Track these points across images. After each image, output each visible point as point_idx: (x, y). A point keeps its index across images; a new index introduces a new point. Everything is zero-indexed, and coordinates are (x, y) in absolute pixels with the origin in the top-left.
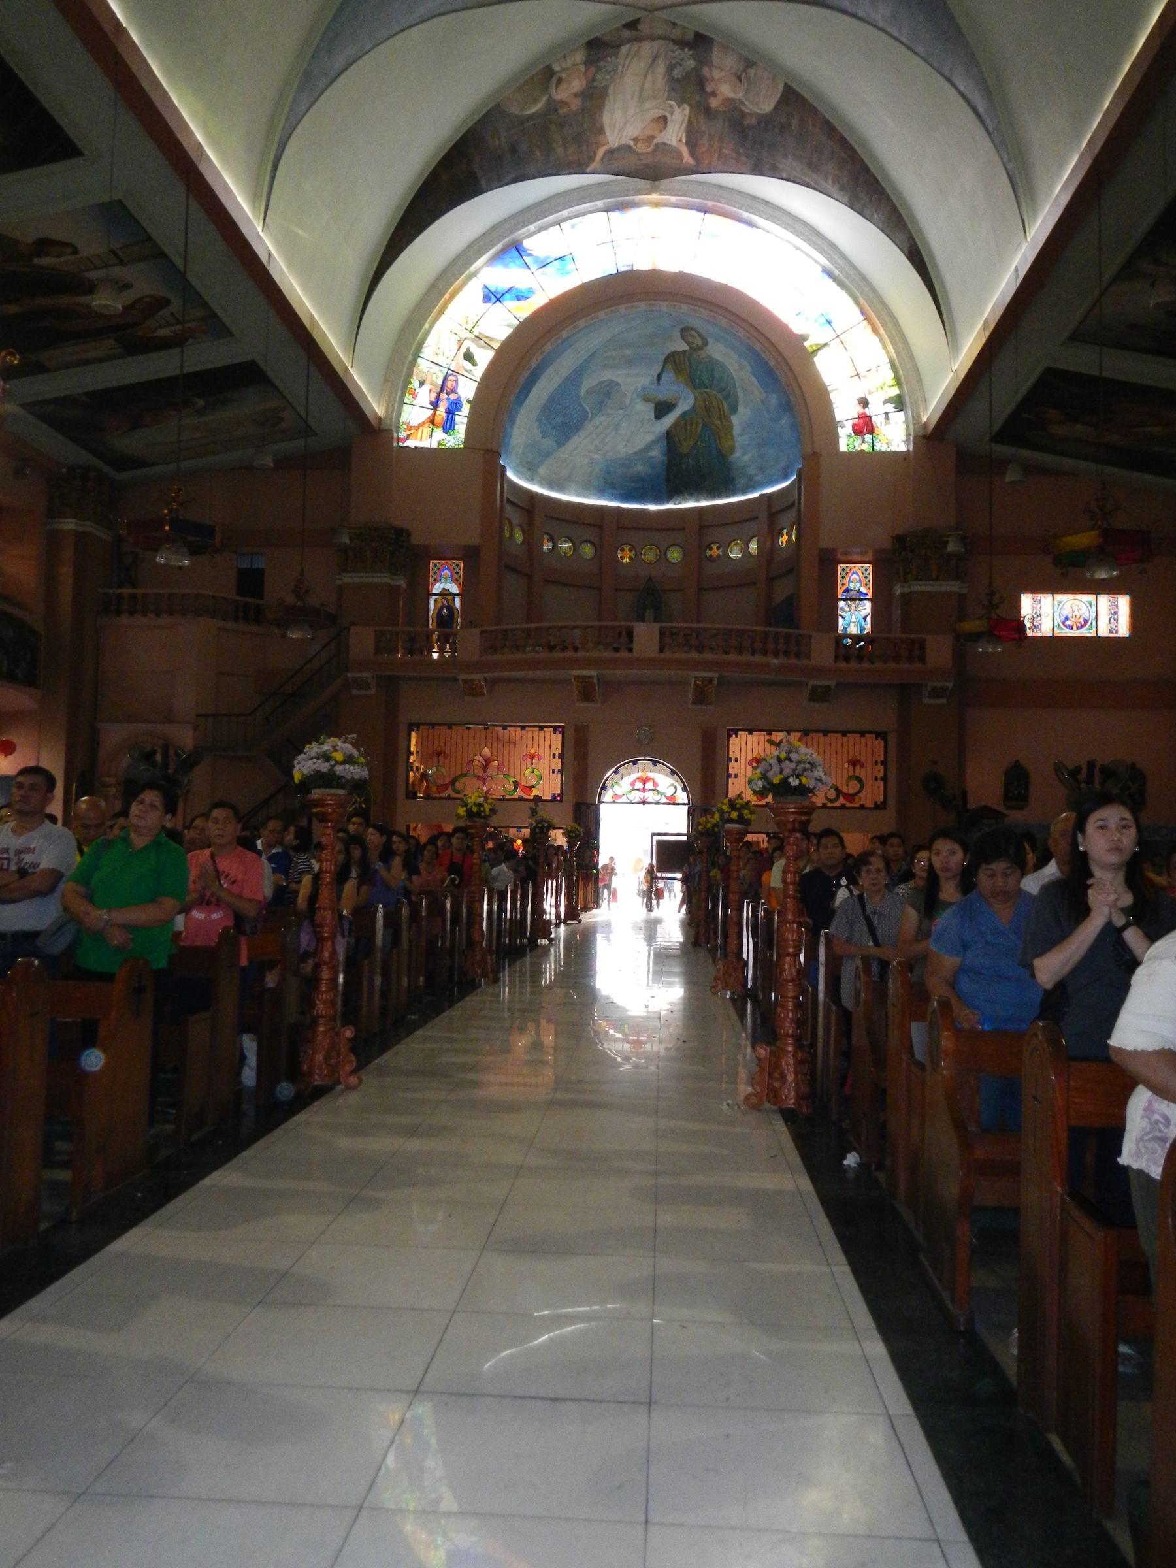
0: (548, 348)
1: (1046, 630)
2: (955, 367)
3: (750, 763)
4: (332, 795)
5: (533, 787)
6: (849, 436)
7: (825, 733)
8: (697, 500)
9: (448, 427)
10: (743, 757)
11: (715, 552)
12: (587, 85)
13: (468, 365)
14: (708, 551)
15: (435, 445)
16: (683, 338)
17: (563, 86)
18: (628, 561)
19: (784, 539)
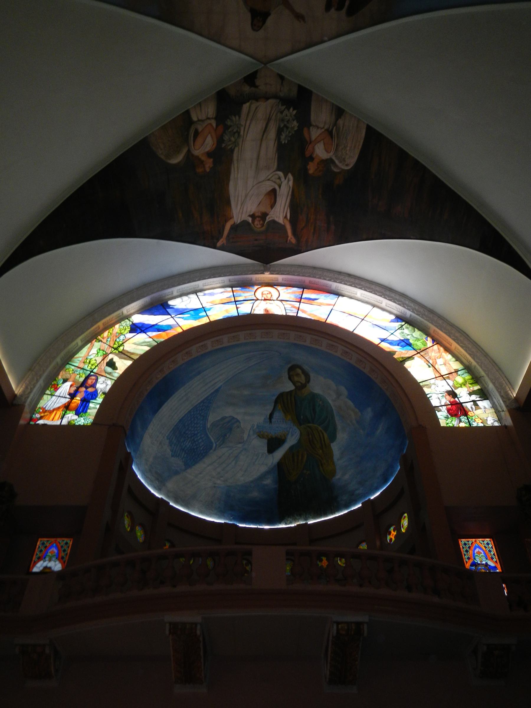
6: (447, 418)
9: (81, 410)
13: (109, 369)
14: (319, 563)
15: (65, 422)
16: (290, 378)
17: (199, 140)
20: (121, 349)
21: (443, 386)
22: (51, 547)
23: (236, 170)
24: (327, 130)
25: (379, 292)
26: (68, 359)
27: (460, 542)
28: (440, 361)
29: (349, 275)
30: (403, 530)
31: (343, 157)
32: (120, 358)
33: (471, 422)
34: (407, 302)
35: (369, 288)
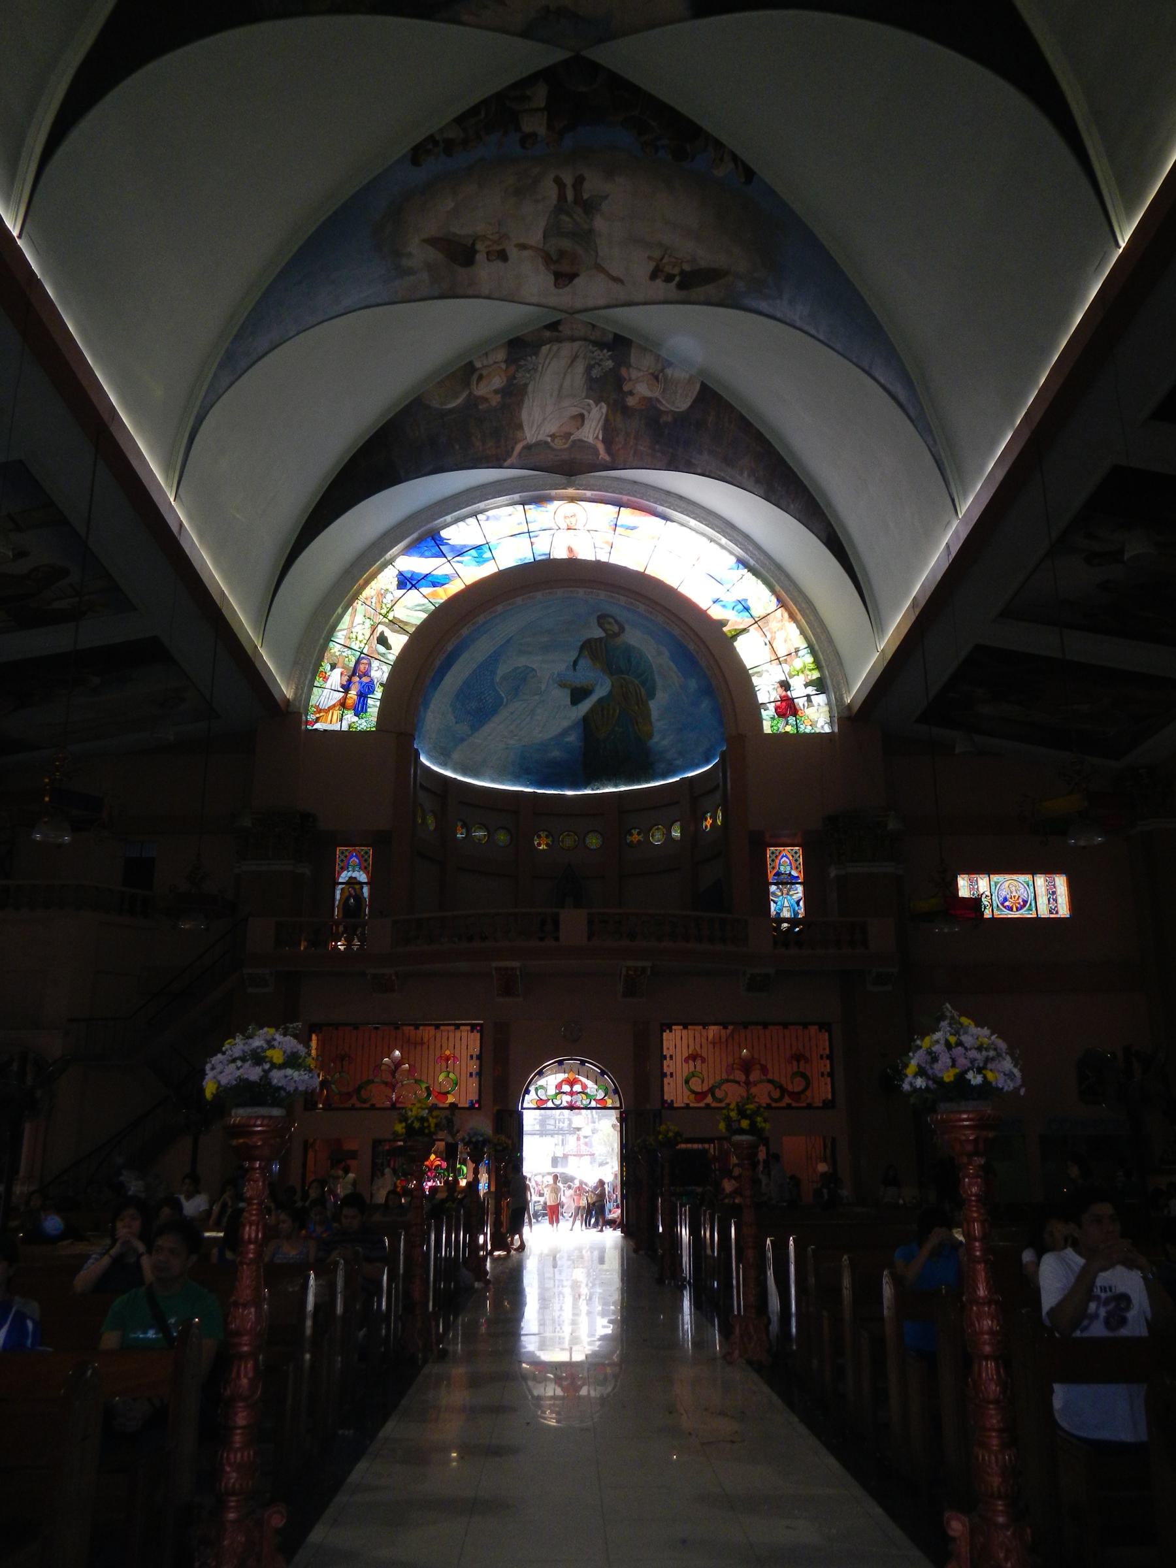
0: (465, 632)
2: (881, 647)
3: (687, 1060)
4: (263, 1117)
5: (448, 1093)
6: (773, 718)
7: (765, 1025)
8: (616, 786)
9: (360, 709)
10: (679, 1054)
11: (635, 837)
12: (507, 381)
13: (381, 649)
15: (345, 728)
16: (600, 625)
17: (483, 384)
18: (545, 848)
19: (709, 822)
20: (390, 617)
24: (652, 374)
25: (717, 527)
27: (768, 851)
29: (681, 498)
32: (394, 631)
33: (799, 725)
35: (705, 520)
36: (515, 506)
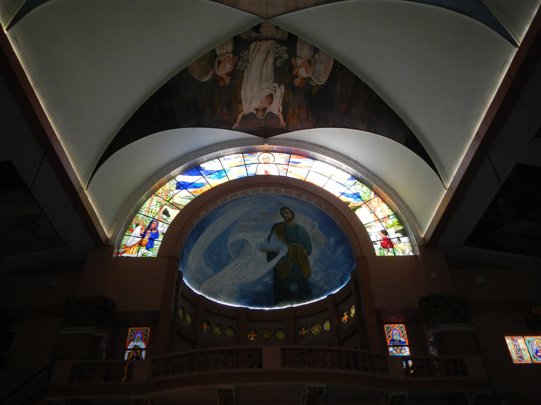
1: (527, 359)
2: (448, 186)
6: (380, 249)
9: (149, 246)
11: (304, 332)
13: (165, 217)
14: (299, 332)
15: (140, 255)
16: (282, 214)
17: (222, 66)
18: (253, 339)
20: (171, 201)
21: (379, 227)
22: (137, 334)
23: (246, 83)
24: (308, 60)
26: (137, 210)
27: (385, 326)
28: (379, 209)
29: (321, 147)
30: (352, 316)
31: (318, 77)
32: (172, 208)
33: (395, 252)
34: (359, 168)
35: (334, 156)
36: (238, 154)
